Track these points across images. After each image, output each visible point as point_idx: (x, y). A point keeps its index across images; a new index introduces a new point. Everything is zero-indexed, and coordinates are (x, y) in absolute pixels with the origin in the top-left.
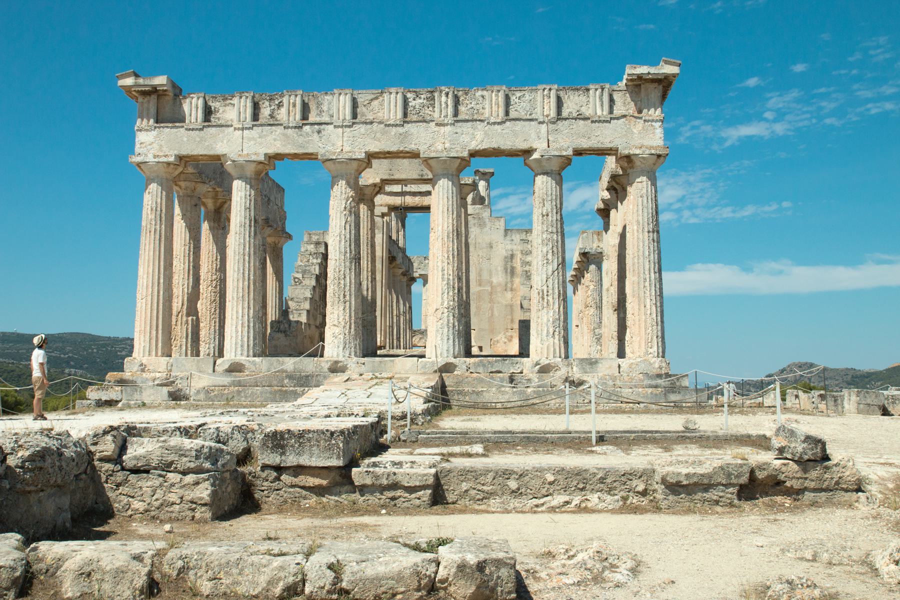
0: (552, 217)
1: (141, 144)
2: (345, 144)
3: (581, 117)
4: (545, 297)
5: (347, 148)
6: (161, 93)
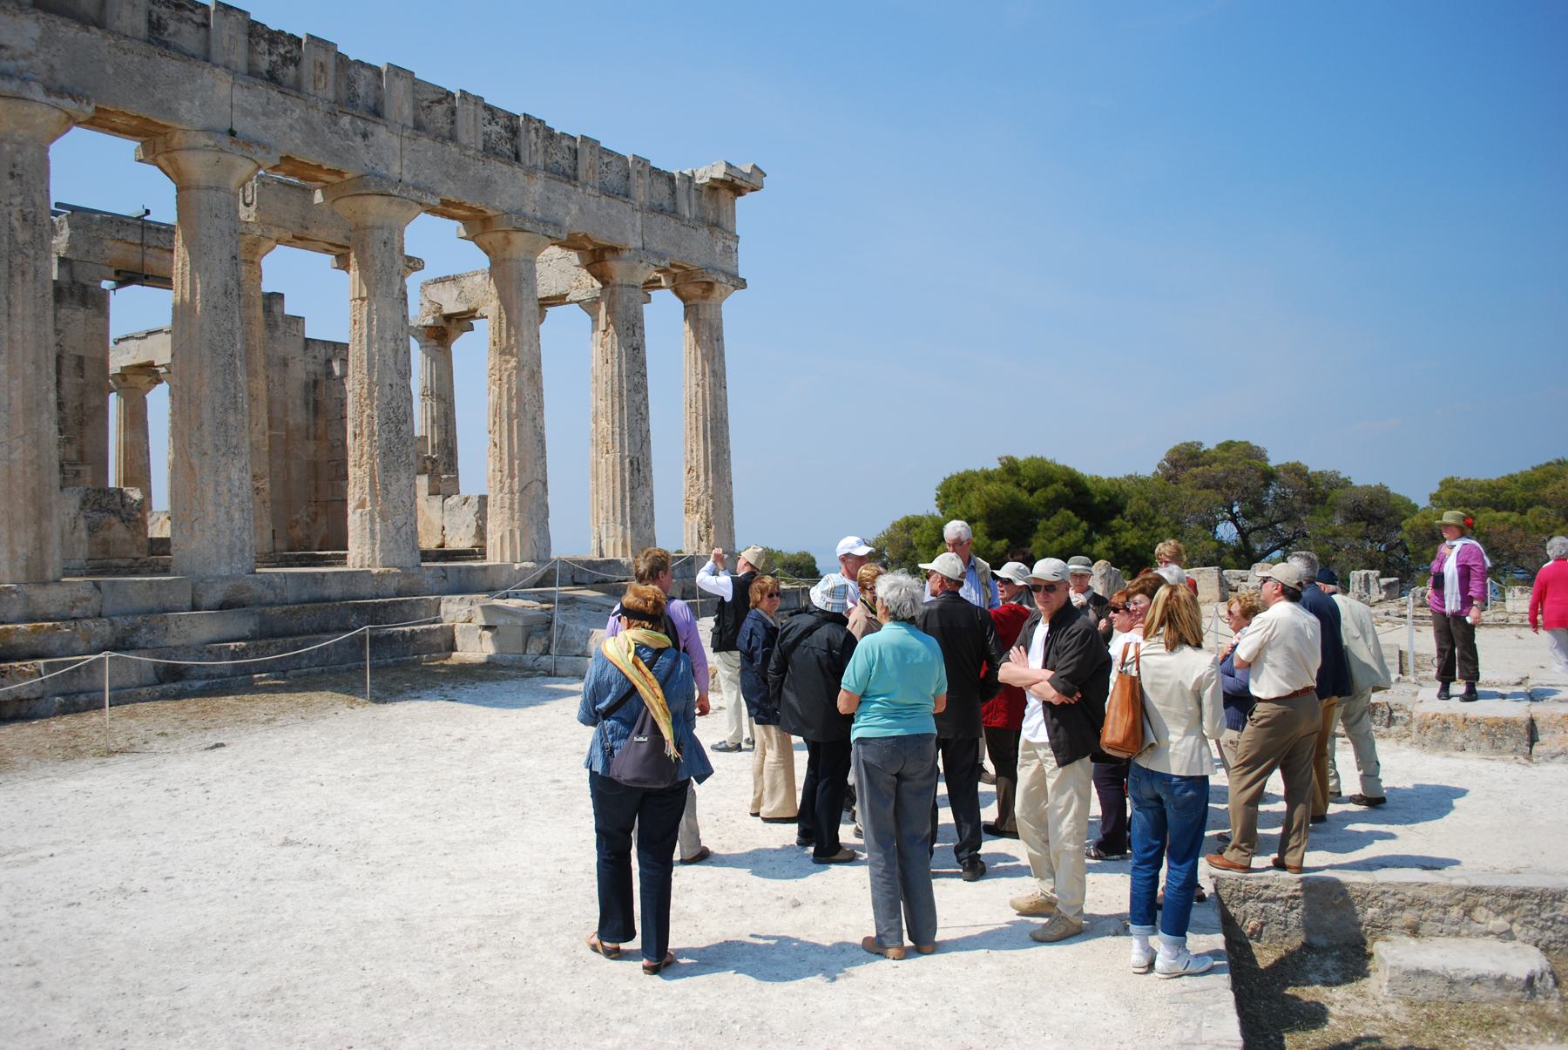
2: (404, 172)
5: (407, 177)
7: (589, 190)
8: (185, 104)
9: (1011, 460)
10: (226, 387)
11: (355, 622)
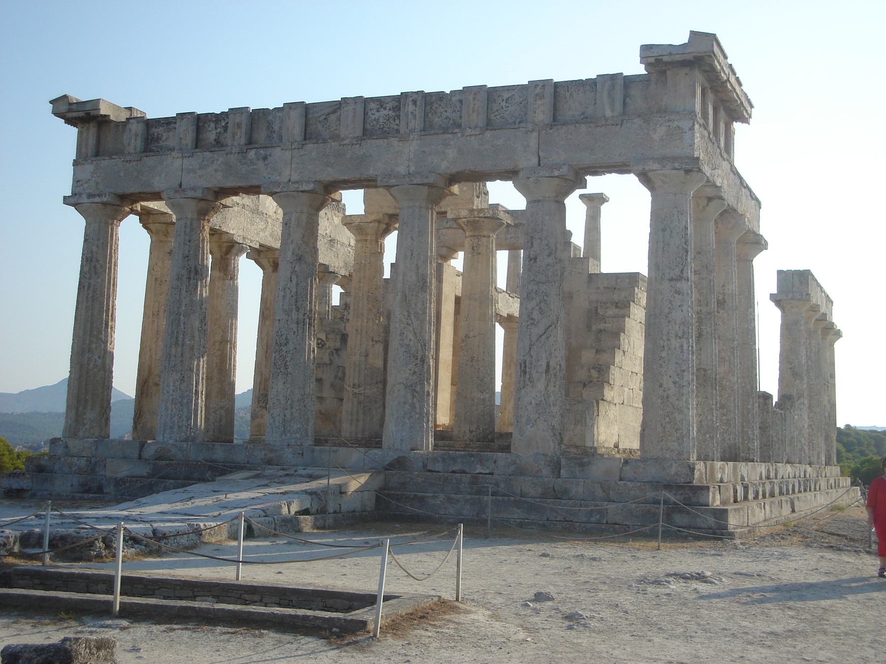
1: (78, 181)
3: (586, 119)
4: (528, 370)
6: (100, 119)
7: (469, 131)
8: (158, 178)
9: (838, 334)
10: (172, 332)
11: (209, 476)
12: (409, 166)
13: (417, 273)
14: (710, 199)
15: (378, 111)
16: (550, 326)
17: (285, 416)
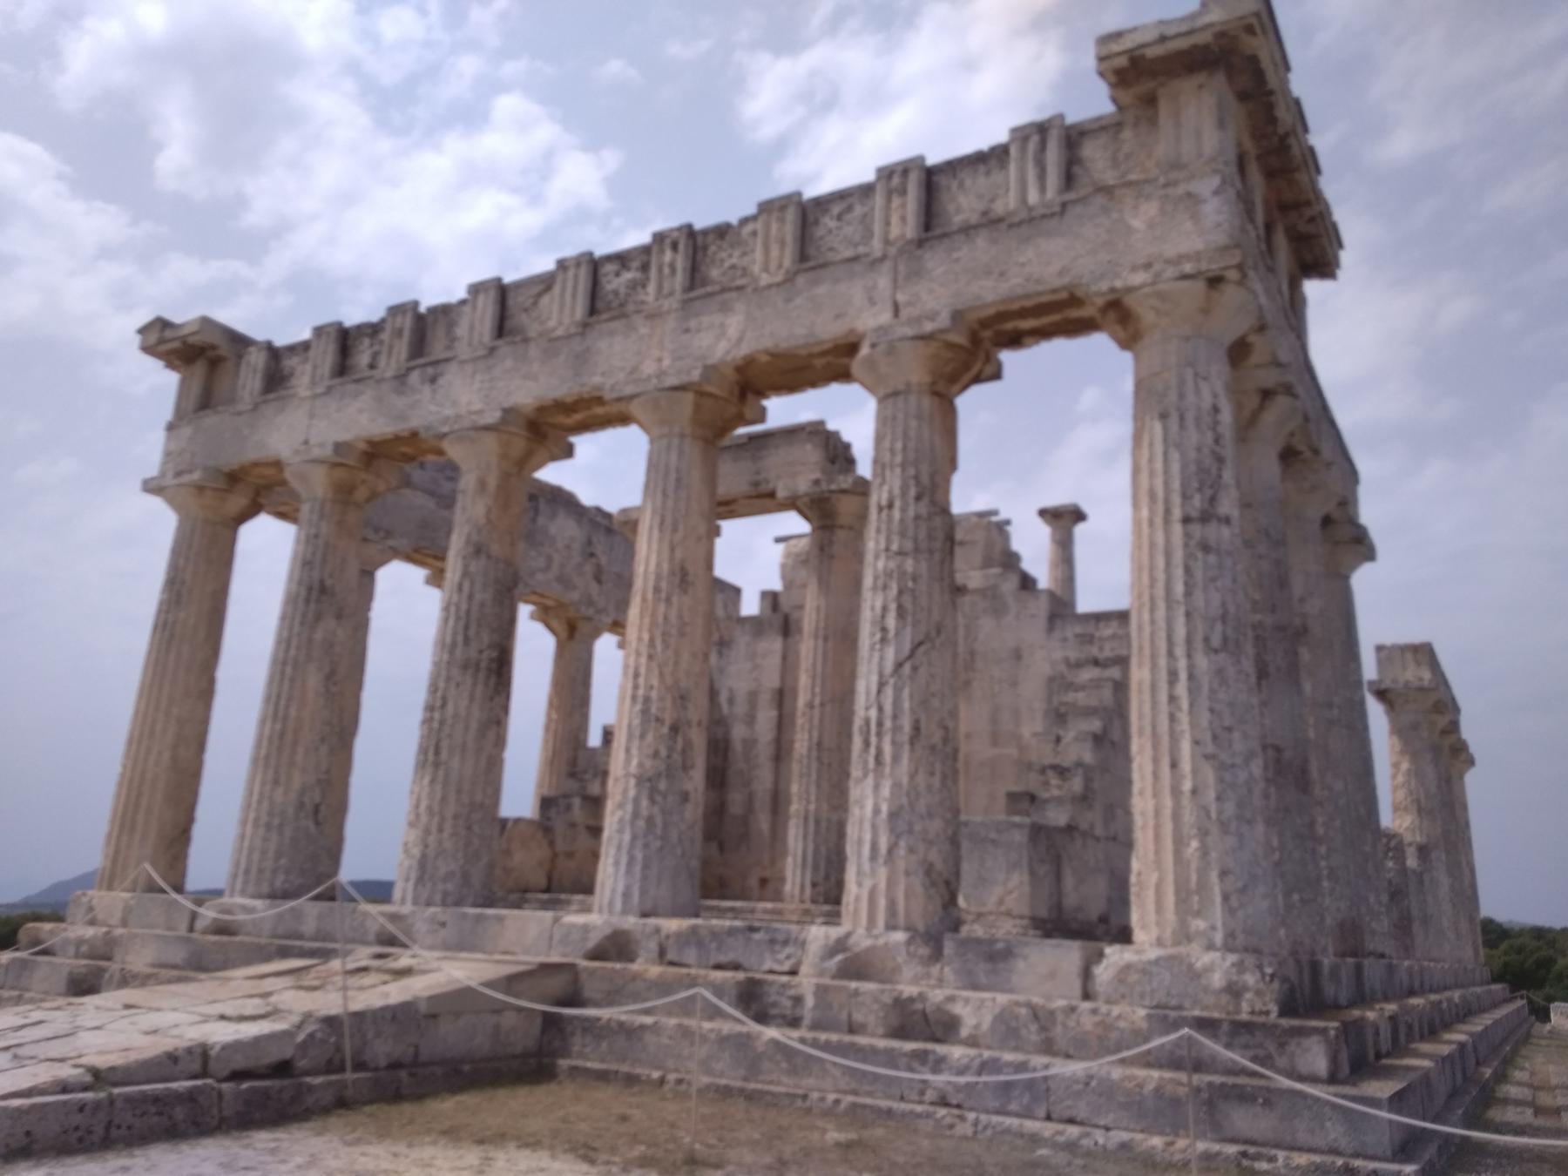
0: (903, 510)
3: (991, 222)
4: (873, 740)
6: (210, 354)
12: (660, 360)
13: (672, 559)
14: (1267, 394)
15: (617, 275)
16: (921, 644)
17: (426, 846)
